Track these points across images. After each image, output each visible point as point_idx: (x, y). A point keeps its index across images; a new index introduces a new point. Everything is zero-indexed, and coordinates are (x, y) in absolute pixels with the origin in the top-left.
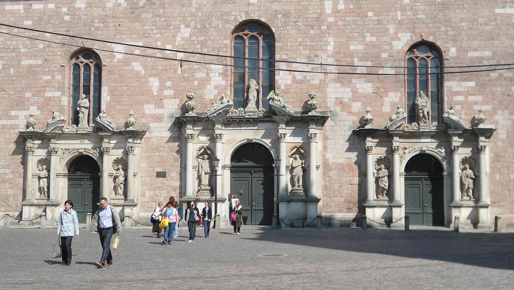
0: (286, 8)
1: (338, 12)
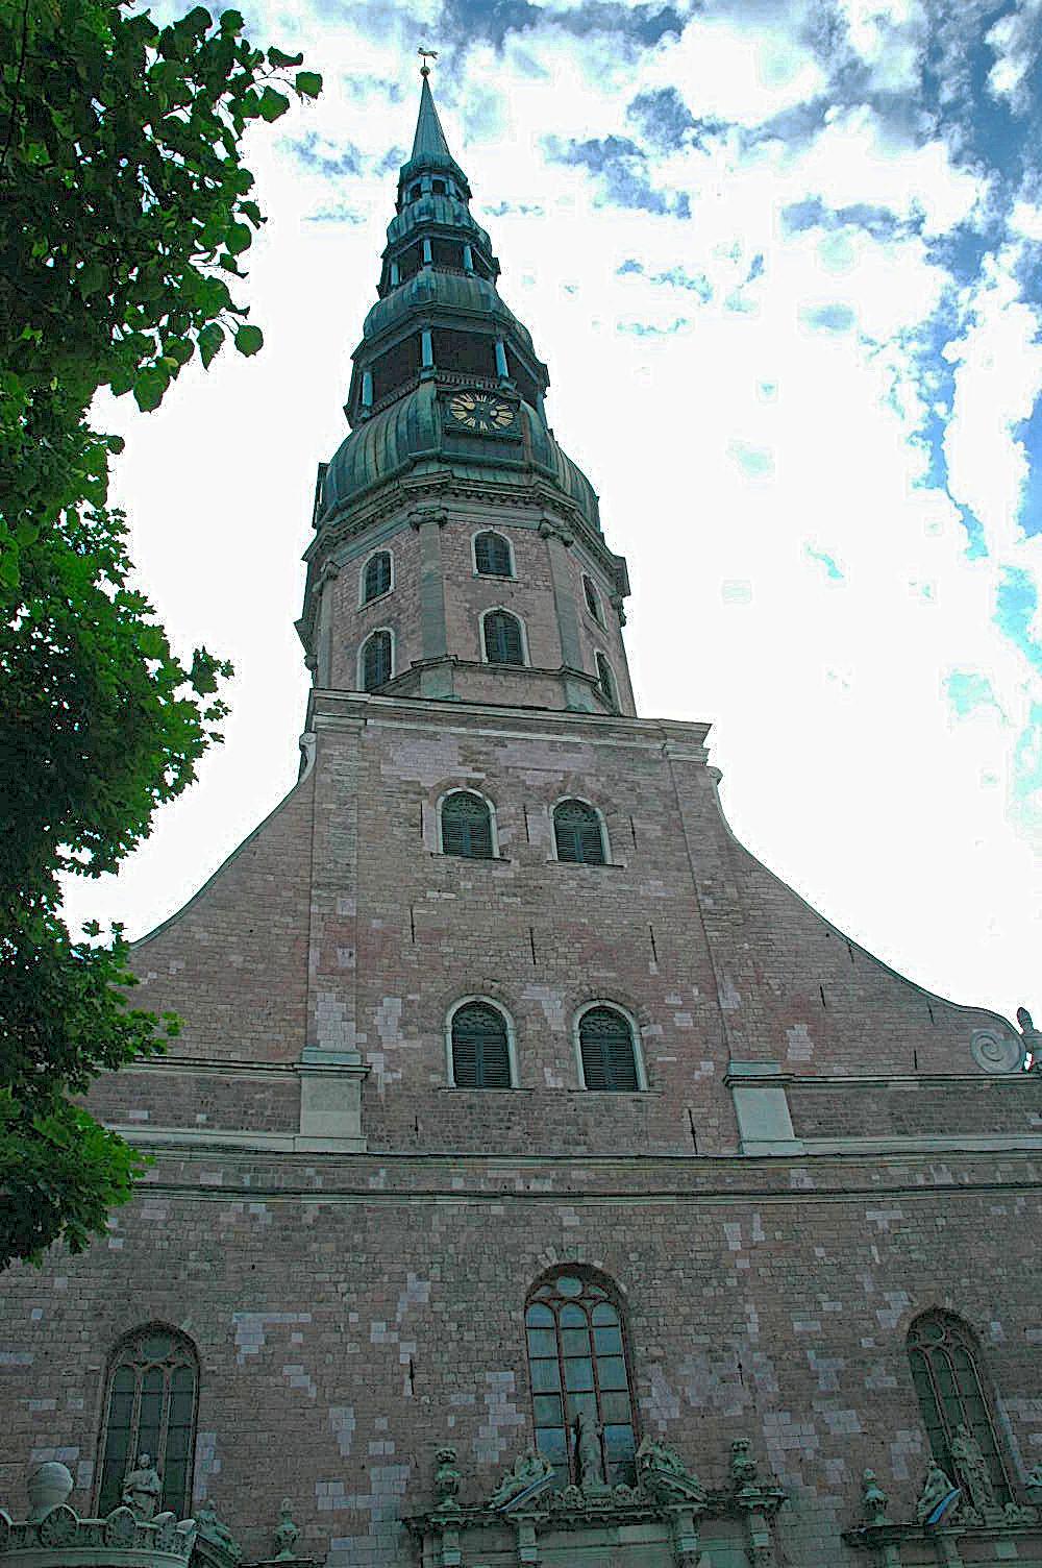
0: (645, 1239)
1: (755, 1248)
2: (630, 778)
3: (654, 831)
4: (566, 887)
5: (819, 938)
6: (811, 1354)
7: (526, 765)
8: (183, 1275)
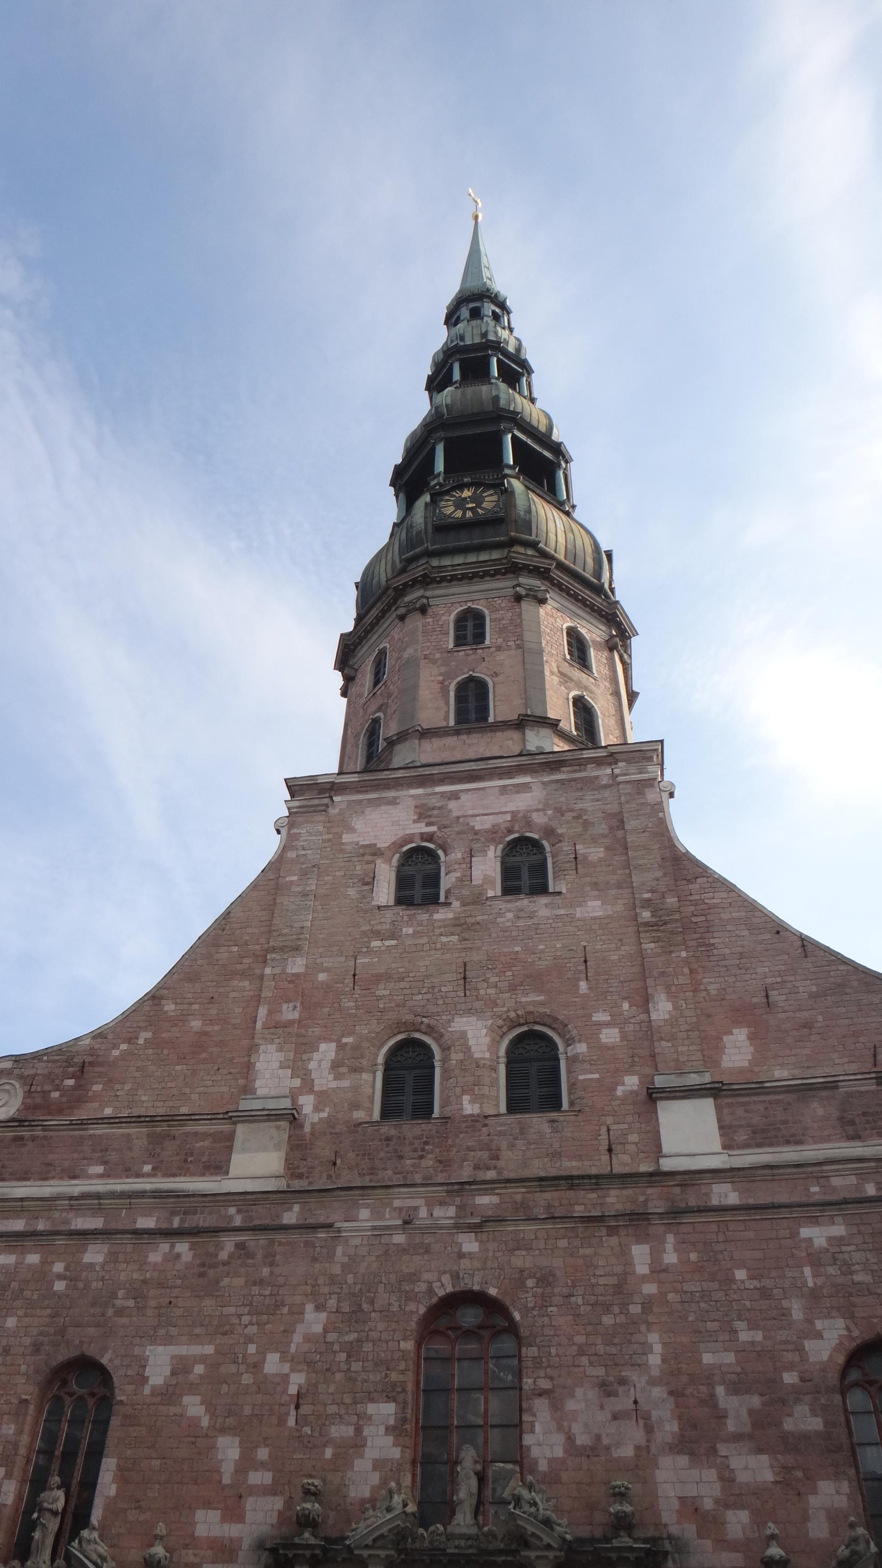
1: (664, 1271)
2: (579, 806)
3: (596, 853)
4: (502, 920)
5: (768, 936)
6: (720, 1390)
7: (475, 812)
8: (110, 1312)
